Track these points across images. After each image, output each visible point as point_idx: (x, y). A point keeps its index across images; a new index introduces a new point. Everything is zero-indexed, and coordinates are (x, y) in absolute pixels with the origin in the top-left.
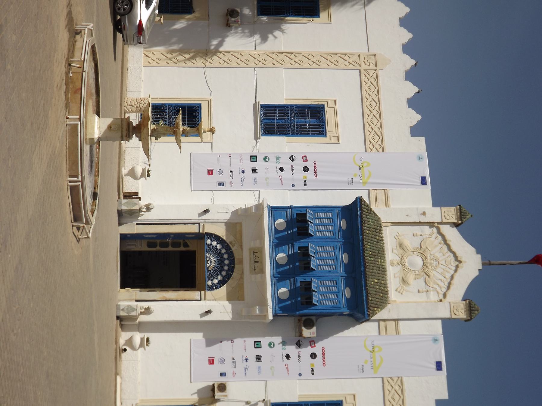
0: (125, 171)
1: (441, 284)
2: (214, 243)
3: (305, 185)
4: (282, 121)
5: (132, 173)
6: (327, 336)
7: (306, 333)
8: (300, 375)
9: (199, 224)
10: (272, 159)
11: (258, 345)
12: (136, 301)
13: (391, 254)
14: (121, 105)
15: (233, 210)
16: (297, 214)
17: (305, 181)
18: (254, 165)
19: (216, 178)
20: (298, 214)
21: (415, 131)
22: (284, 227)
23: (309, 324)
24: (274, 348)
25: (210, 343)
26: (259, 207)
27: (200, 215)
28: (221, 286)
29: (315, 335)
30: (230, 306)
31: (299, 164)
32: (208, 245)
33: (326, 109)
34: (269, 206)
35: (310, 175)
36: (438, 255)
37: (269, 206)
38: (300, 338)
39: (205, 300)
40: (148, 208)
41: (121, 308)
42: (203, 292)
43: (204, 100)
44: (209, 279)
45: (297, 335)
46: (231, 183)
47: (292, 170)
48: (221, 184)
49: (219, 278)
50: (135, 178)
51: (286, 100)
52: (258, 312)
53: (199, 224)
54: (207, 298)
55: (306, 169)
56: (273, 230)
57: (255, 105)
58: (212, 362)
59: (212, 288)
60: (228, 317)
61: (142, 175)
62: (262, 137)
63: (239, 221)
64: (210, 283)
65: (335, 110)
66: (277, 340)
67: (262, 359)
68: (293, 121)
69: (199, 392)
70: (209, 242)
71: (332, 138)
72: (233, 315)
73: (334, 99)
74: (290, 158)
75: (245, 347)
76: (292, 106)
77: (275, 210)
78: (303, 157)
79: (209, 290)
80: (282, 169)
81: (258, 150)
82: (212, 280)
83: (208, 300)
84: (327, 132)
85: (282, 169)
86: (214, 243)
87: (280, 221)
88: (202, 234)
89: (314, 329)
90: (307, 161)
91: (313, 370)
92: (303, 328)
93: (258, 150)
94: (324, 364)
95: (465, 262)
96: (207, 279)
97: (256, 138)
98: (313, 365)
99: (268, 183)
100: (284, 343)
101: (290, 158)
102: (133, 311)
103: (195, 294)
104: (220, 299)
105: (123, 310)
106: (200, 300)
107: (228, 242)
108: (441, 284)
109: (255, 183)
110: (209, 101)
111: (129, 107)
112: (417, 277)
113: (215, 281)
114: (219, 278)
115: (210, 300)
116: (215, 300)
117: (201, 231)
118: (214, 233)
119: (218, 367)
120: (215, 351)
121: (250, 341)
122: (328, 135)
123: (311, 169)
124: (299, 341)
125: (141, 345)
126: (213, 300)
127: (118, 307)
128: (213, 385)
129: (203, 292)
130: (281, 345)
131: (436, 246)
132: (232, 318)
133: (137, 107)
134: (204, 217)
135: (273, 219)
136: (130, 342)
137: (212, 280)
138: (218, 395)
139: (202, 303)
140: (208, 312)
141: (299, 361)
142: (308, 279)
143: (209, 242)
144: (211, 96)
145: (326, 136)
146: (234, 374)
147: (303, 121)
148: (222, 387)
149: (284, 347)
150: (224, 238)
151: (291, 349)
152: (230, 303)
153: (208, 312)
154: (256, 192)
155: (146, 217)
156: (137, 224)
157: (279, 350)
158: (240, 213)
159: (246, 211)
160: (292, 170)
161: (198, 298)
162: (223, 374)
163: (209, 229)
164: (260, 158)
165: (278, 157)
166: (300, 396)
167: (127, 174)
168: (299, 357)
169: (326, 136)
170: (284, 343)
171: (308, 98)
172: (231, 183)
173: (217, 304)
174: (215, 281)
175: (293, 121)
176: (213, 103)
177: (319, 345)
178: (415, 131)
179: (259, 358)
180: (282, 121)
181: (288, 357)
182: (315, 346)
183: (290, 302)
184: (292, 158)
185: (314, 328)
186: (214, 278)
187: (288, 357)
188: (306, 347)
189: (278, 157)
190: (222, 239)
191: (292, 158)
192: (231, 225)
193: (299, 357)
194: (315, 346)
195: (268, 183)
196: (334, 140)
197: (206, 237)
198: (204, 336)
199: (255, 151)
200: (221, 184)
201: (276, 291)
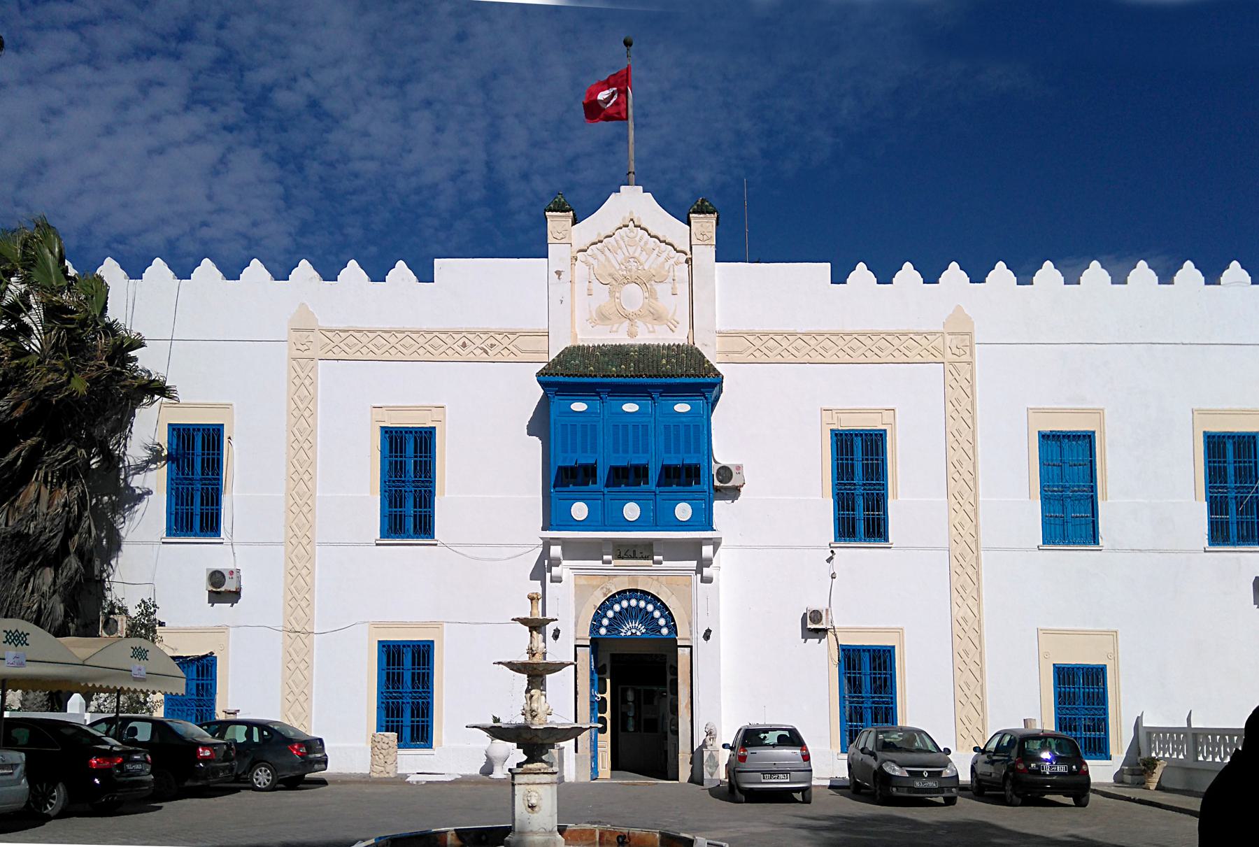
1: (664, 255)
13: (617, 336)
21: (425, 274)
36: (620, 257)
54: (688, 636)
59: (673, 628)
64: (665, 631)
70: (603, 631)
79: (676, 633)
95: (631, 213)
103: (683, 653)
108: (664, 255)
110: (377, 625)
112: (652, 294)
131: (607, 259)
143: (603, 631)
178: (425, 274)
196: (436, 414)
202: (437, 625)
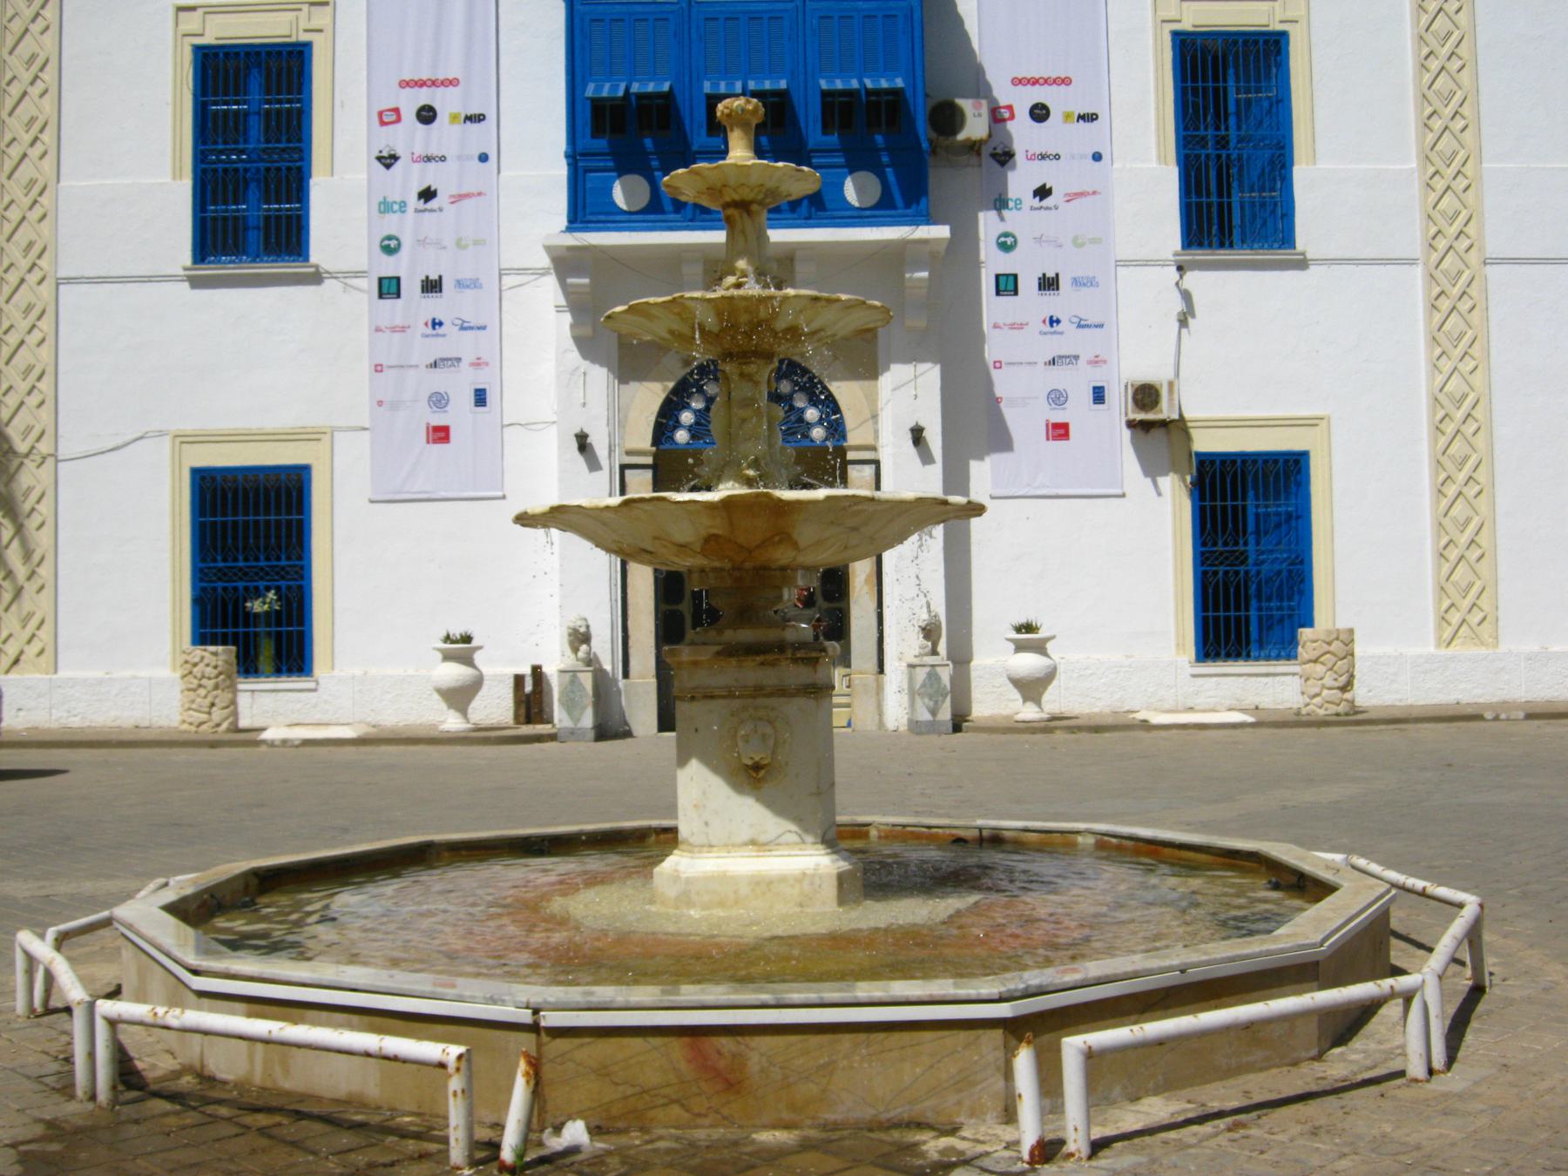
0: (452, 722)
2: (687, 417)
3: (477, 118)
4: (254, 192)
5: (459, 697)
6: (979, 71)
7: (975, 126)
8: (1097, 157)
9: (623, 468)
10: (391, 224)
11: (1007, 285)
12: (881, 670)
14: (214, 744)
15: (575, 354)
16: (594, 136)
17: (469, 118)
18: (411, 287)
19: (460, 415)
20: (597, 131)
22: (640, 185)
23: (947, 118)
24: (1016, 233)
25: (1000, 440)
26: (565, 263)
27: (593, 464)
28: (830, 397)
29: (984, 102)
30: (895, 368)
31: (408, 137)
32: (693, 437)
33: (209, 39)
34: (569, 229)
35: (446, 102)
37: (569, 229)
38: (986, 151)
39: (874, 449)
40: (580, 638)
41: (925, 716)
42: (851, 456)
43: (177, 459)
44: (806, 436)
45: (974, 160)
46: (478, 364)
47: (429, 159)
48: (480, 398)
49: (800, 402)
50: (476, 685)
51: (177, 174)
52: (925, 274)
53: (623, 468)
54: (870, 441)
55: (427, 115)
56: (652, 217)
57: (196, 283)
58: (1060, 431)
59: (836, 429)
60: (930, 375)
61: (467, 659)
62: (314, 259)
63: (613, 335)
64: (818, 433)
65: (212, 10)
66: (988, 224)
67: (1051, 274)
68: (254, 156)
69: (1151, 470)
71: (314, 24)
72: (923, 360)
73: (171, 12)
74: (388, 166)
75: (1013, 326)
76: (200, 157)
77: (585, 208)
78: (383, 123)
79: (844, 437)
80: (427, 195)
81: (358, 274)
82: (809, 426)
83: (877, 438)
84: (293, 39)
85: (427, 195)
86: (687, 417)
87: (619, 196)
88: (656, 456)
89: (966, 104)
90: (396, 110)
91: (1082, 117)
92: (961, 136)
93: (358, 274)
94: (1066, 81)
96: (806, 443)
97: (316, 278)
98: (1067, 117)
99: (476, 243)
100: (1000, 203)
101: (388, 166)
102: (938, 678)
104: (872, 399)
105: (934, 712)
106: (877, 463)
107: (681, 373)
109: (475, 284)
110: (185, 440)
111: (217, 714)
113: (812, 414)
114: (800, 402)
115: (876, 432)
116: (875, 417)
117: (649, 460)
118: (653, 419)
119: (1078, 412)
120: (1025, 419)
121: (993, 308)
122: (304, 37)
123: (424, 97)
124: (994, 156)
125: (1040, 648)
126: (876, 423)
127: (915, 727)
128: (1131, 424)
129: (851, 456)
130: (1005, 212)
132: (935, 362)
133: (216, 687)
134: (601, 451)
135: (610, 218)
136: (1031, 688)
137: (809, 426)
138: (1165, 411)
139: (885, 456)
140: (917, 435)
141: (1057, 157)
142: (815, 109)
143: (682, 436)
144: (161, 434)
145: (308, 46)
146: (1096, 361)
147: (255, 127)
148: (1146, 395)
149: (1011, 204)
150: (671, 385)
151: (1020, 182)
152: (888, 369)
153: (917, 435)
154: (508, 281)
155: (604, 646)
156: (626, 675)
157: (1022, 219)
158: (587, 331)
159: (582, 307)
160: (429, 159)
161: (869, 471)
162: (1099, 395)
163: (641, 437)
164: (388, 266)
165: (386, 207)
166: (1161, 159)
167: (463, 712)
168: (1043, 157)
169: (308, 46)
170: (1000, 203)
171: (169, 98)
172: (478, 364)
173: (892, 410)
174: (812, 414)
175: (254, 156)
176: (189, 426)
177: (1004, 93)
179: (1049, 284)
180: (254, 192)
181: (1043, 192)
182: (1010, 108)
183: (889, 170)
184: (388, 161)
185: (960, 102)
186: (801, 420)
187: (1043, 192)
188: (1009, 136)
189: (386, 207)
190: (674, 391)
191: (388, 161)
192: (629, 361)
193: (1043, 157)
194: (1010, 108)
195: (476, 243)
197: (667, 446)
198: (981, 458)
199: (362, 283)
200: (480, 398)
201: (855, 213)
202: (311, 436)
